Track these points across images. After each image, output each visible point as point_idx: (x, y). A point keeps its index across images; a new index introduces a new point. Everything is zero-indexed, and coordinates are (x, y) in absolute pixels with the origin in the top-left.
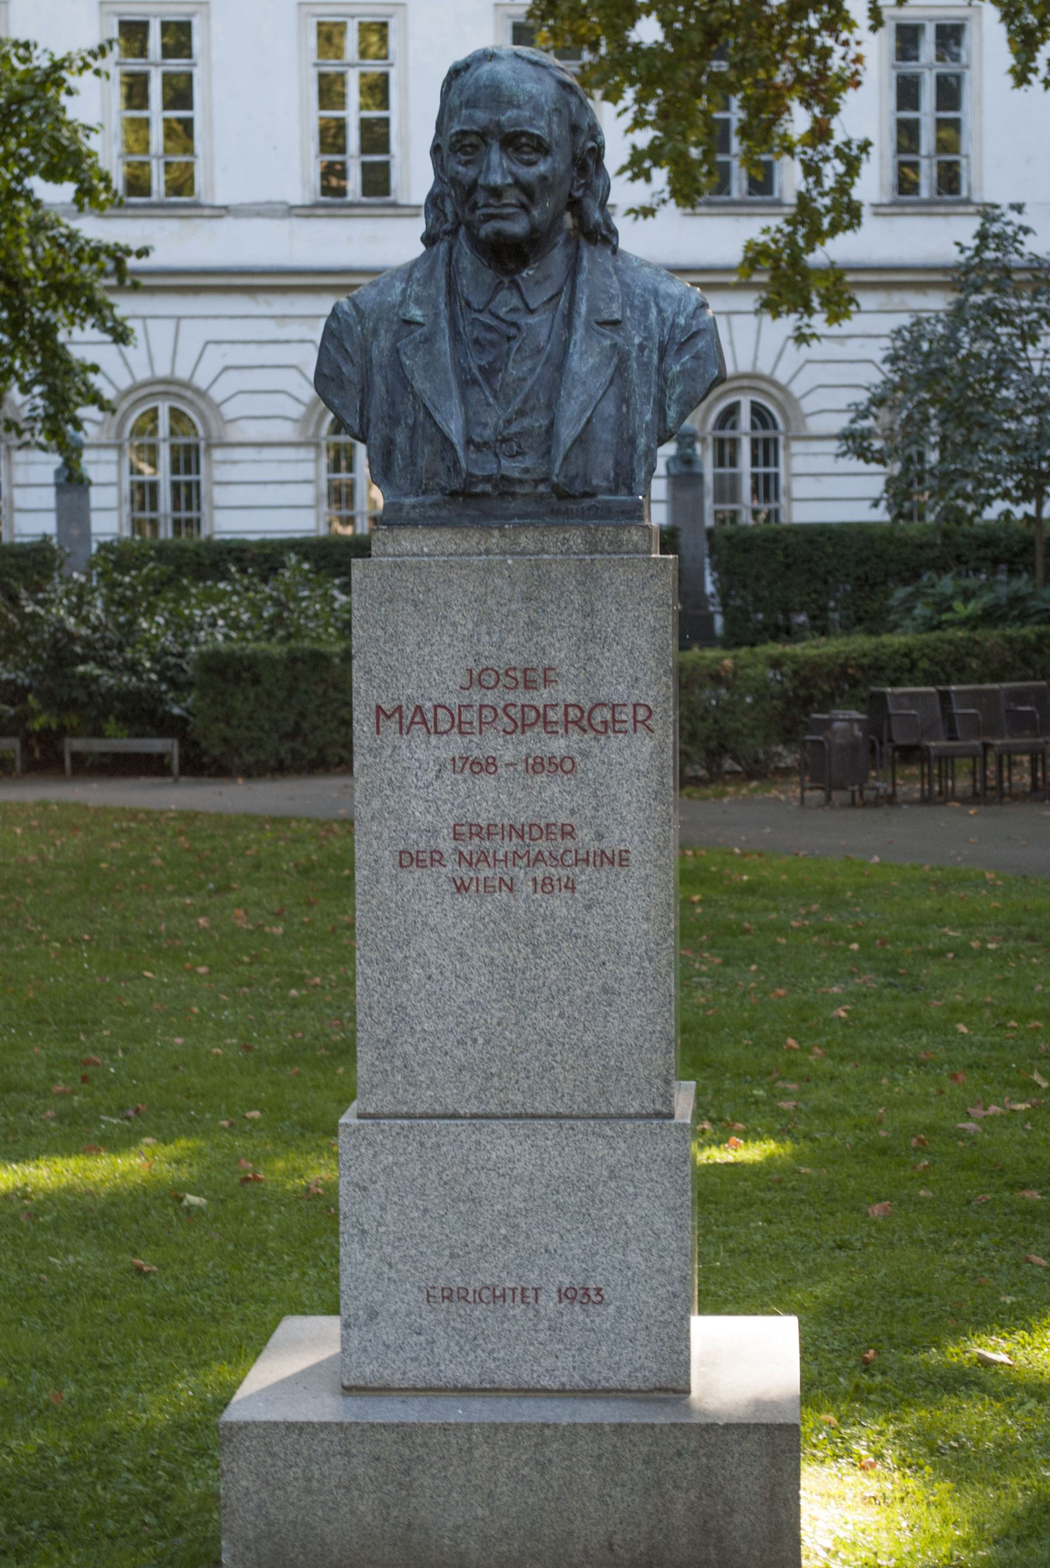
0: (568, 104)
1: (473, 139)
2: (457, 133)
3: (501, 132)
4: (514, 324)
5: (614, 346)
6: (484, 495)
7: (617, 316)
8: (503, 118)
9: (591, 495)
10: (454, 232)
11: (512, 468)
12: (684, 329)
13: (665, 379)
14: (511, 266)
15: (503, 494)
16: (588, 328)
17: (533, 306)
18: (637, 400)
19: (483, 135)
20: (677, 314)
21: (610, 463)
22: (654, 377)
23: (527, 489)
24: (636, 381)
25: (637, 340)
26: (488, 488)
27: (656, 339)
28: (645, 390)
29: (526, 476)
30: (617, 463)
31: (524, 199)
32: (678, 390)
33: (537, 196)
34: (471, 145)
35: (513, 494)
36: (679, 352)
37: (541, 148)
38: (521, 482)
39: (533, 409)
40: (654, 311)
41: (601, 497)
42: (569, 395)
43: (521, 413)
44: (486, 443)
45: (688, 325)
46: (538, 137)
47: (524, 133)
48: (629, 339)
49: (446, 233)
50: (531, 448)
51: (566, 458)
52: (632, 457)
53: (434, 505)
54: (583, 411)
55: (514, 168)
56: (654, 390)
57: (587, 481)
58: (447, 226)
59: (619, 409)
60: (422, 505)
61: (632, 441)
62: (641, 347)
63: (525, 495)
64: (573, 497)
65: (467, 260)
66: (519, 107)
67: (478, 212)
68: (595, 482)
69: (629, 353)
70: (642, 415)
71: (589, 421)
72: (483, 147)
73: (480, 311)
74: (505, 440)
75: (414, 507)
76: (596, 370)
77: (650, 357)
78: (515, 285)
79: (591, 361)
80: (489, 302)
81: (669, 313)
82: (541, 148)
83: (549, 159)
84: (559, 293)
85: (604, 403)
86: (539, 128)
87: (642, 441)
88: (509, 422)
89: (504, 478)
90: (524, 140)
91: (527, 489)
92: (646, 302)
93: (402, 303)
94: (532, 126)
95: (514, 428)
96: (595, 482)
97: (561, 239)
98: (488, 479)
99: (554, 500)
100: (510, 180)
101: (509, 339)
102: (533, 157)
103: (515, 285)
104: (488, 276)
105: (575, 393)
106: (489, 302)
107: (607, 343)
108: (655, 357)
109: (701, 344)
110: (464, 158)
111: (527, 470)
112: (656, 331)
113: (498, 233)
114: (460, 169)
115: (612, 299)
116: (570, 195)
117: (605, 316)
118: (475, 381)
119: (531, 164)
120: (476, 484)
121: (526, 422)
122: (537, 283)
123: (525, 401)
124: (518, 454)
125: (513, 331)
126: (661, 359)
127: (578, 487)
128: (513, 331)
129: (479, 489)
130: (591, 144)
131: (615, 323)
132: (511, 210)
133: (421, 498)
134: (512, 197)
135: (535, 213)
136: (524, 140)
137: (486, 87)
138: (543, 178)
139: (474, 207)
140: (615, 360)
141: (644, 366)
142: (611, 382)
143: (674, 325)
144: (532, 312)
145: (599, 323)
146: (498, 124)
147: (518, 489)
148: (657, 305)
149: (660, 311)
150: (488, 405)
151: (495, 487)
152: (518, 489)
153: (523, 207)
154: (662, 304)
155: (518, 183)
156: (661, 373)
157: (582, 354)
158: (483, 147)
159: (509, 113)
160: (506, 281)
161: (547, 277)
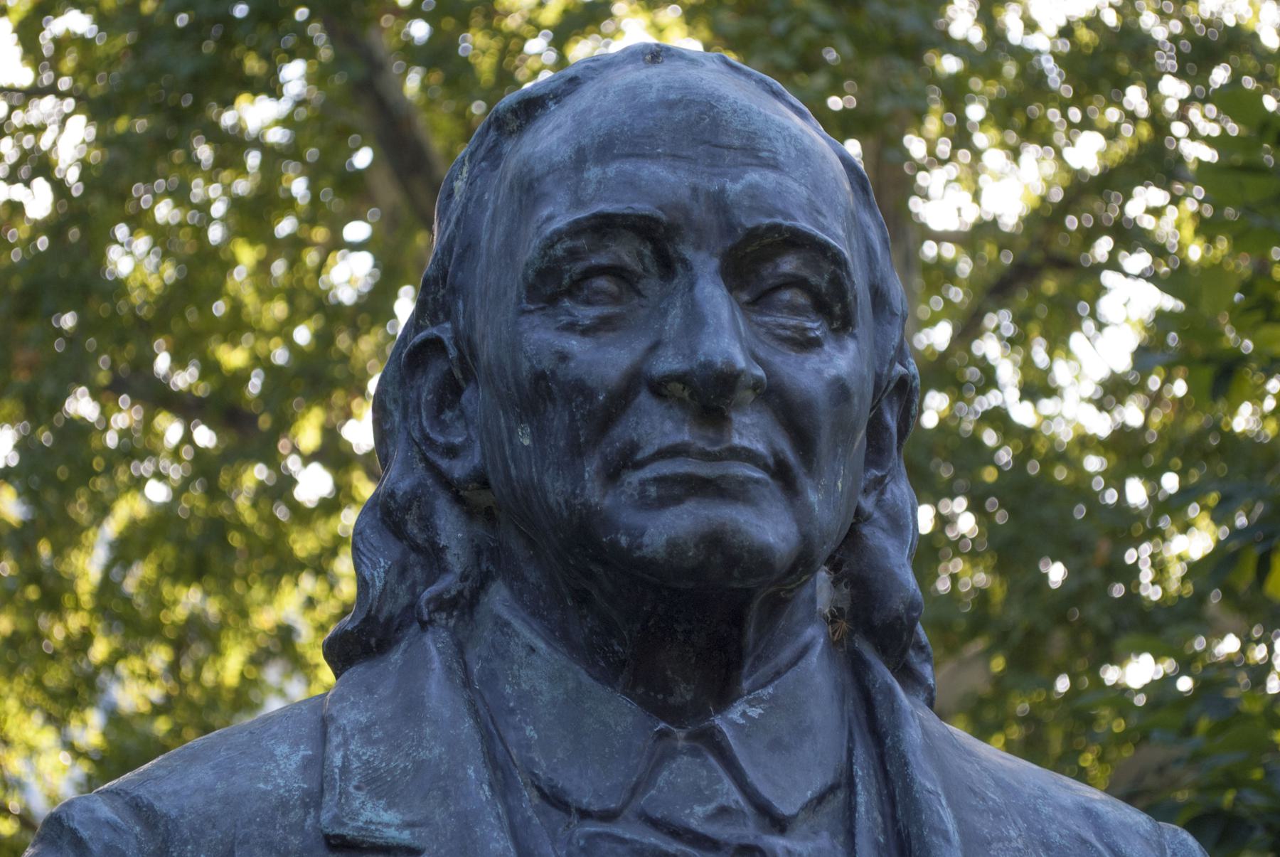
1: (624, 252)
2: (576, 230)
3: (729, 228)
8: (734, 188)
10: (464, 605)
17: (786, 808)
19: (659, 238)
34: (616, 272)
46: (837, 260)
47: (796, 241)
49: (441, 604)
58: (447, 584)
65: (537, 668)
66: (775, 166)
67: (633, 478)
72: (652, 285)
73: (608, 816)
80: (634, 791)
84: (847, 782)
86: (836, 237)
93: (314, 800)
97: (815, 633)
102: (815, 327)
104: (618, 713)
106: (634, 791)
110: (587, 314)
113: (715, 541)
114: (574, 344)
119: (807, 344)
134: (751, 431)
136: (789, 264)
137: (671, 105)
139: (627, 460)
144: (780, 824)
146: (719, 203)
153: (781, 473)
158: (652, 285)
159: (753, 176)
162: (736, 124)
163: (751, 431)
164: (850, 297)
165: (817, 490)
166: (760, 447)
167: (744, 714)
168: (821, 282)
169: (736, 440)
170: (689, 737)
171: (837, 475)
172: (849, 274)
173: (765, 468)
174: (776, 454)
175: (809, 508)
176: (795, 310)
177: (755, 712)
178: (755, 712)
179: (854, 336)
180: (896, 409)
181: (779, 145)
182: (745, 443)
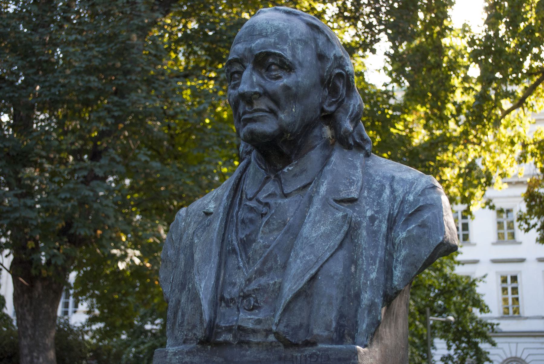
0: (315, 40)
4: (267, 204)
5: (345, 217)
6: (227, 343)
7: (355, 195)
8: (253, 45)
9: (313, 344)
11: (247, 319)
12: (411, 204)
13: (393, 244)
14: (279, 166)
15: (241, 343)
16: (325, 203)
18: (363, 263)
20: (408, 193)
21: (333, 316)
22: (382, 242)
23: (259, 338)
24: (365, 245)
25: (369, 213)
26: (229, 337)
27: (387, 212)
28: (372, 253)
29: (258, 327)
30: (341, 316)
31: (272, 105)
32: (403, 253)
33: (282, 102)
35: (248, 343)
36: (407, 222)
37: (287, 67)
38: (254, 331)
39: (270, 269)
40: (387, 191)
41: (320, 346)
42: (297, 255)
43: (260, 273)
44: (232, 299)
45: (416, 201)
46: (280, 56)
47: (269, 54)
48: (361, 213)
50: (265, 302)
51: (287, 309)
52: (357, 311)
53: (189, 353)
54: (306, 270)
55: (263, 82)
56: (381, 253)
57: (308, 330)
59: (347, 269)
60: (181, 352)
61: (358, 296)
62: (372, 219)
63: (258, 344)
64: (296, 345)
66: (266, 36)
68: (316, 332)
69: (359, 223)
70: (367, 274)
71: (313, 278)
74: (246, 296)
75: (175, 354)
76: (327, 236)
77: (379, 226)
78: (278, 179)
79: (323, 229)
81: (400, 191)
82: (287, 67)
83: (293, 75)
85: (331, 262)
86: (283, 50)
87: (366, 297)
88: (249, 280)
89: (240, 328)
90: (271, 60)
91: (259, 338)
92: (383, 186)
94: (278, 49)
95: (253, 286)
96: (316, 332)
98: (229, 330)
99: (282, 348)
100: (257, 89)
101: (263, 215)
102: (280, 73)
103: (278, 179)
105: (302, 254)
107: (340, 214)
108: (384, 227)
109: (426, 215)
111: (259, 322)
112: (387, 206)
115: (352, 183)
116: (323, 110)
117: (343, 195)
118: (234, 251)
120: (220, 334)
121: (263, 280)
122: (295, 175)
123: (264, 263)
124: (254, 308)
125: (264, 210)
126: (390, 229)
127: (302, 336)
128: (264, 210)
129: (221, 339)
130: (337, 71)
131: (352, 201)
132: (261, 114)
133: (181, 347)
135: (282, 116)
136: (271, 60)
138: (286, 88)
140: (345, 228)
141: (373, 234)
142: (341, 246)
143: (402, 202)
144: (286, 196)
145: (336, 201)
146: (251, 50)
147: (253, 339)
148: (391, 186)
149: (393, 191)
150: (239, 268)
151: (235, 336)
152: (253, 339)
153: (272, 111)
154: (395, 186)
155: (266, 94)
156: (388, 238)
157: (315, 223)
160: (273, 177)
161: (302, 171)
162: (259, 29)
163: (262, 104)
164: (287, 63)
165: (283, 113)
166: (263, 107)
167: (288, 170)
168: (278, 62)
169: (255, 107)
170: (275, 177)
171: (292, 108)
172: (285, 58)
173: (266, 112)
174: (269, 108)
175: (281, 118)
176: (275, 70)
177: (290, 168)
178: (290, 168)
179: (295, 72)
180: (342, 81)
181: (269, 30)
182: (258, 107)
